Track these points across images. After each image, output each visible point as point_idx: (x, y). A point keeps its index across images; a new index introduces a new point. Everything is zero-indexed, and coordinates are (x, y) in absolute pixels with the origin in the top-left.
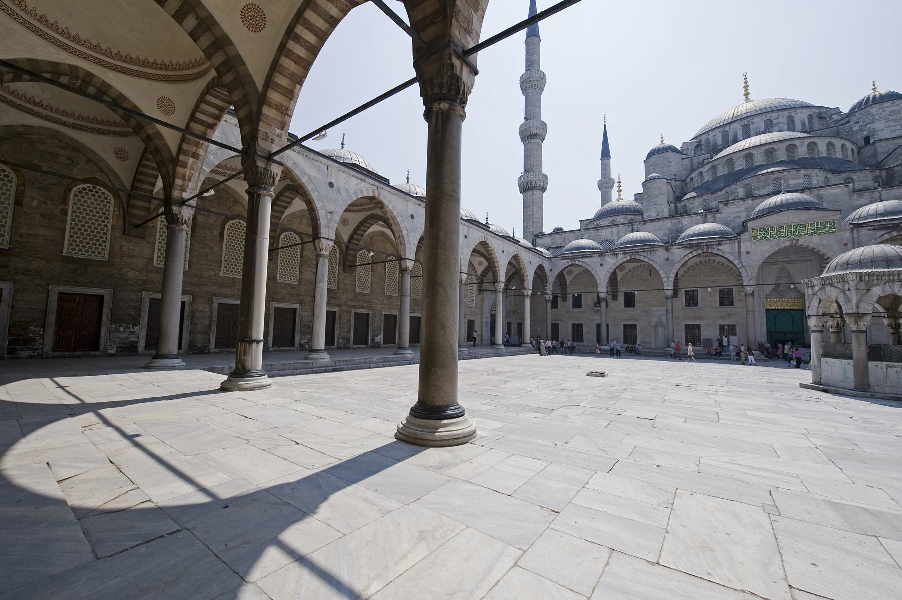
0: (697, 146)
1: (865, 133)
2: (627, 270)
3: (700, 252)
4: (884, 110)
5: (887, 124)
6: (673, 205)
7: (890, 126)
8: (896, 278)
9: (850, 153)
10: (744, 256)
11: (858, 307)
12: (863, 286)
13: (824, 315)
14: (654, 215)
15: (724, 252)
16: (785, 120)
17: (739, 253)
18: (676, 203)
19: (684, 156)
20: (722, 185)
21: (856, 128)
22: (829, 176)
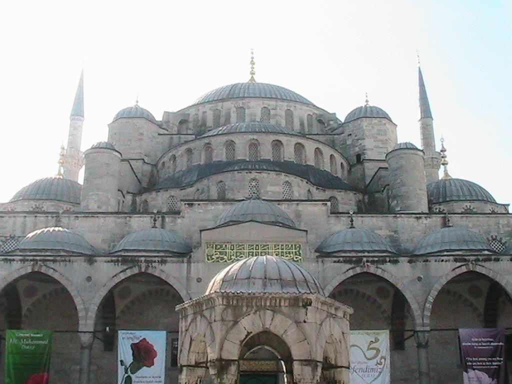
0: (182, 122)
1: (357, 149)
2: (39, 295)
3: (136, 270)
4: (373, 127)
5: (374, 144)
6: (129, 198)
7: (377, 147)
8: (268, 304)
9: (339, 168)
10: (194, 283)
11: (221, 349)
12: (230, 317)
13: (197, 365)
14: (93, 207)
15: (168, 276)
16: (283, 114)
17: (188, 279)
18: (134, 195)
19: (162, 132)
20: (195, 179)
21: (349, 142)
22: (313, 189)
